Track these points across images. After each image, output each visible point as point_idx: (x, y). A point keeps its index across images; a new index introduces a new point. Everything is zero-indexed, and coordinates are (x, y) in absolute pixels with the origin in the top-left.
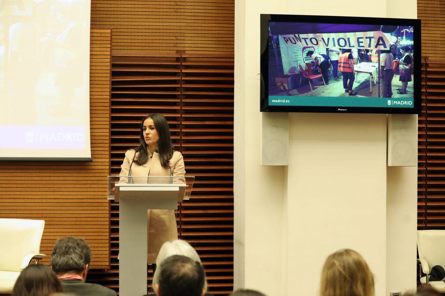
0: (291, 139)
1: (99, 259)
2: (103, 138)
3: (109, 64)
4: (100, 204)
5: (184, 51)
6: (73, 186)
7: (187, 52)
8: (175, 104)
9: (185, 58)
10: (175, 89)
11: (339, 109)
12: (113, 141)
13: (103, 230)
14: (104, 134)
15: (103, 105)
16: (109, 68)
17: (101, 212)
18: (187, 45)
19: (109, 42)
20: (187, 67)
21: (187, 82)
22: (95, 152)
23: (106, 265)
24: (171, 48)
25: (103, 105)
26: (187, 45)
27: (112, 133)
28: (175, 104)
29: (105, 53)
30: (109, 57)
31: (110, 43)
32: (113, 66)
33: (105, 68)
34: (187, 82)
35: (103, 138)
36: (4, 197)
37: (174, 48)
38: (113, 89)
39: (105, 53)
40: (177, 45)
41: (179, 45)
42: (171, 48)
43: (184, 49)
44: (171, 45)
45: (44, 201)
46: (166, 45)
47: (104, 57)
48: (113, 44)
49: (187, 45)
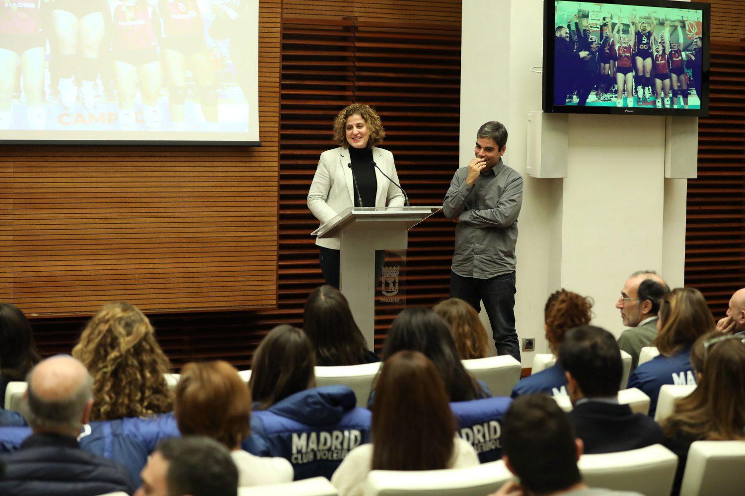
0: (569, 144)
1: (264, 297)
2: (271, 134)
3: (279, 35)
4: (267, 224)
5: (356, 18)
6: (232, 199)
7: (360, 19)
8: (343, 88)
9: (357, 27)
10: (344, 69)
11: (627, 110)
12: (283, 137)
13: (269, 258)
14: (272, 129)
15: (271, 89)
16: (278, 40)
17: (267, 233)
18: (356, 9)
19: (279, 5)
20: (360, 40)
21: (360, 59)
22: (261, 153)
23: (272, 305)
24: (337, 13)
25: (271, 89)
26: (356, 9)
27: (283, 127)
28: (343, 88)
29: (274, 20)
30: (279, 25)
31: (280, 7)
32: (284, 36)
33: (275, 40)
34: (360, 59)
35: (271, 134)
36: (144, 216)
37: (341, 13)
38: (284, 68)
39: (274, 20)
40: (343, 9)
41: (347, 9)
42: (337, 13)
43: (352, 14)
44: (336, 8)
45: (195, 220)
46: (330, 8)
47: (272, 25)
48: (285, 6)
49: (356, 9)
